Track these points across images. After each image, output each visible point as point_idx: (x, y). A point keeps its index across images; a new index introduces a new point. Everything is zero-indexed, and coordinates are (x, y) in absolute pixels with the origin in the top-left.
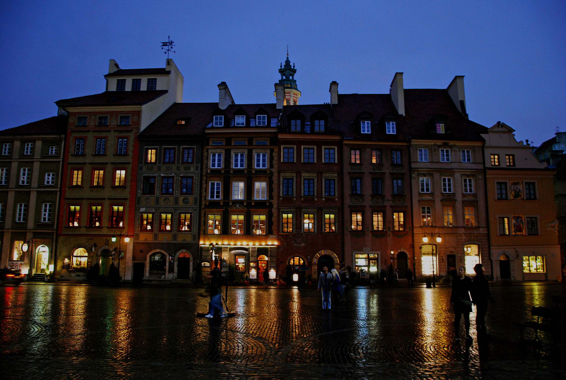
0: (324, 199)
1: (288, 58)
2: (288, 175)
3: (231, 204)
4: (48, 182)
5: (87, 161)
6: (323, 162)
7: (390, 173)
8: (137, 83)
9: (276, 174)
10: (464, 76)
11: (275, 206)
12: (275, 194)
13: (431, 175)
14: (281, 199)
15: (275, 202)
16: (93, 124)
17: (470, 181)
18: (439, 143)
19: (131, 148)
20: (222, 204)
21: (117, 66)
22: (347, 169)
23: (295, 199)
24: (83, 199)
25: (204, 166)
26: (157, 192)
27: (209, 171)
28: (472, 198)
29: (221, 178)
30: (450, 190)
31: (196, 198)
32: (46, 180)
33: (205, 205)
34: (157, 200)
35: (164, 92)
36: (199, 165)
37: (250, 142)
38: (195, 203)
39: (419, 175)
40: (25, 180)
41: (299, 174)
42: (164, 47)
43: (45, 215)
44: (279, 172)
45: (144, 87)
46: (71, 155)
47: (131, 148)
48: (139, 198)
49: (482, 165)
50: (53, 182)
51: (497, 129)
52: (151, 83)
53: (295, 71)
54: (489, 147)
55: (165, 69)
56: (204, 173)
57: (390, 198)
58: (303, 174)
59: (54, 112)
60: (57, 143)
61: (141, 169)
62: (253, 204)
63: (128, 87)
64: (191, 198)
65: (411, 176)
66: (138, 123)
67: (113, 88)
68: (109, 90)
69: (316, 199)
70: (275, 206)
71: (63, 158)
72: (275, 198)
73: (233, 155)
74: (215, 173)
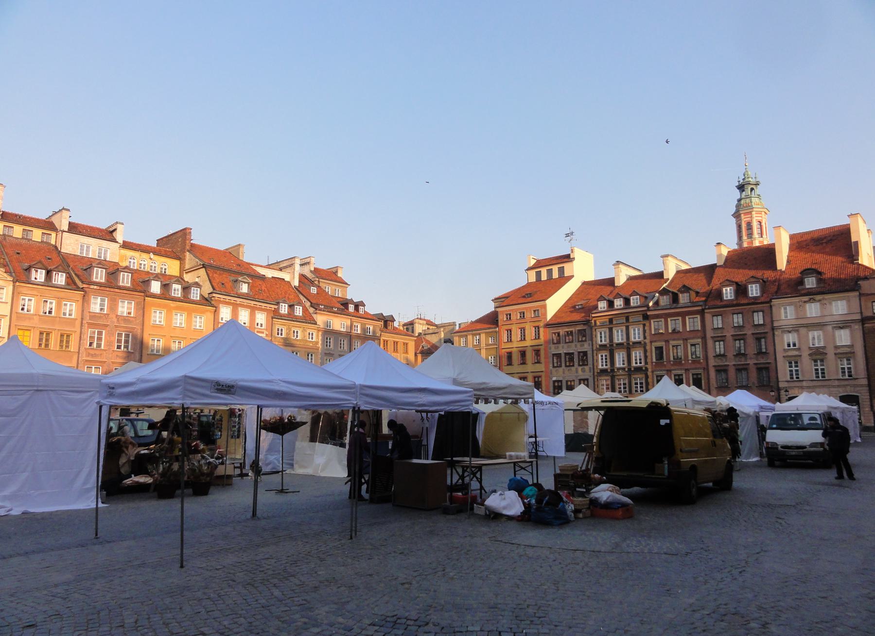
8: (550, 272)
11: (650, 370)
12: (649, 360)
13: (797, 331)
15: (649, 366)
18: (806, 298)
22: (710, 333)
26: (563, 365)
35: (572, 277)
37: (627, 319)
41: (667, 341)
44: (651, 342)
45: (555, 275)
52: (561, 270)
53: (757, 184)
59: (490, 308)
63: (544, 277)
64: (586, 368)
65: (774, 334)
66: (545, 314)
74: (603, 347)
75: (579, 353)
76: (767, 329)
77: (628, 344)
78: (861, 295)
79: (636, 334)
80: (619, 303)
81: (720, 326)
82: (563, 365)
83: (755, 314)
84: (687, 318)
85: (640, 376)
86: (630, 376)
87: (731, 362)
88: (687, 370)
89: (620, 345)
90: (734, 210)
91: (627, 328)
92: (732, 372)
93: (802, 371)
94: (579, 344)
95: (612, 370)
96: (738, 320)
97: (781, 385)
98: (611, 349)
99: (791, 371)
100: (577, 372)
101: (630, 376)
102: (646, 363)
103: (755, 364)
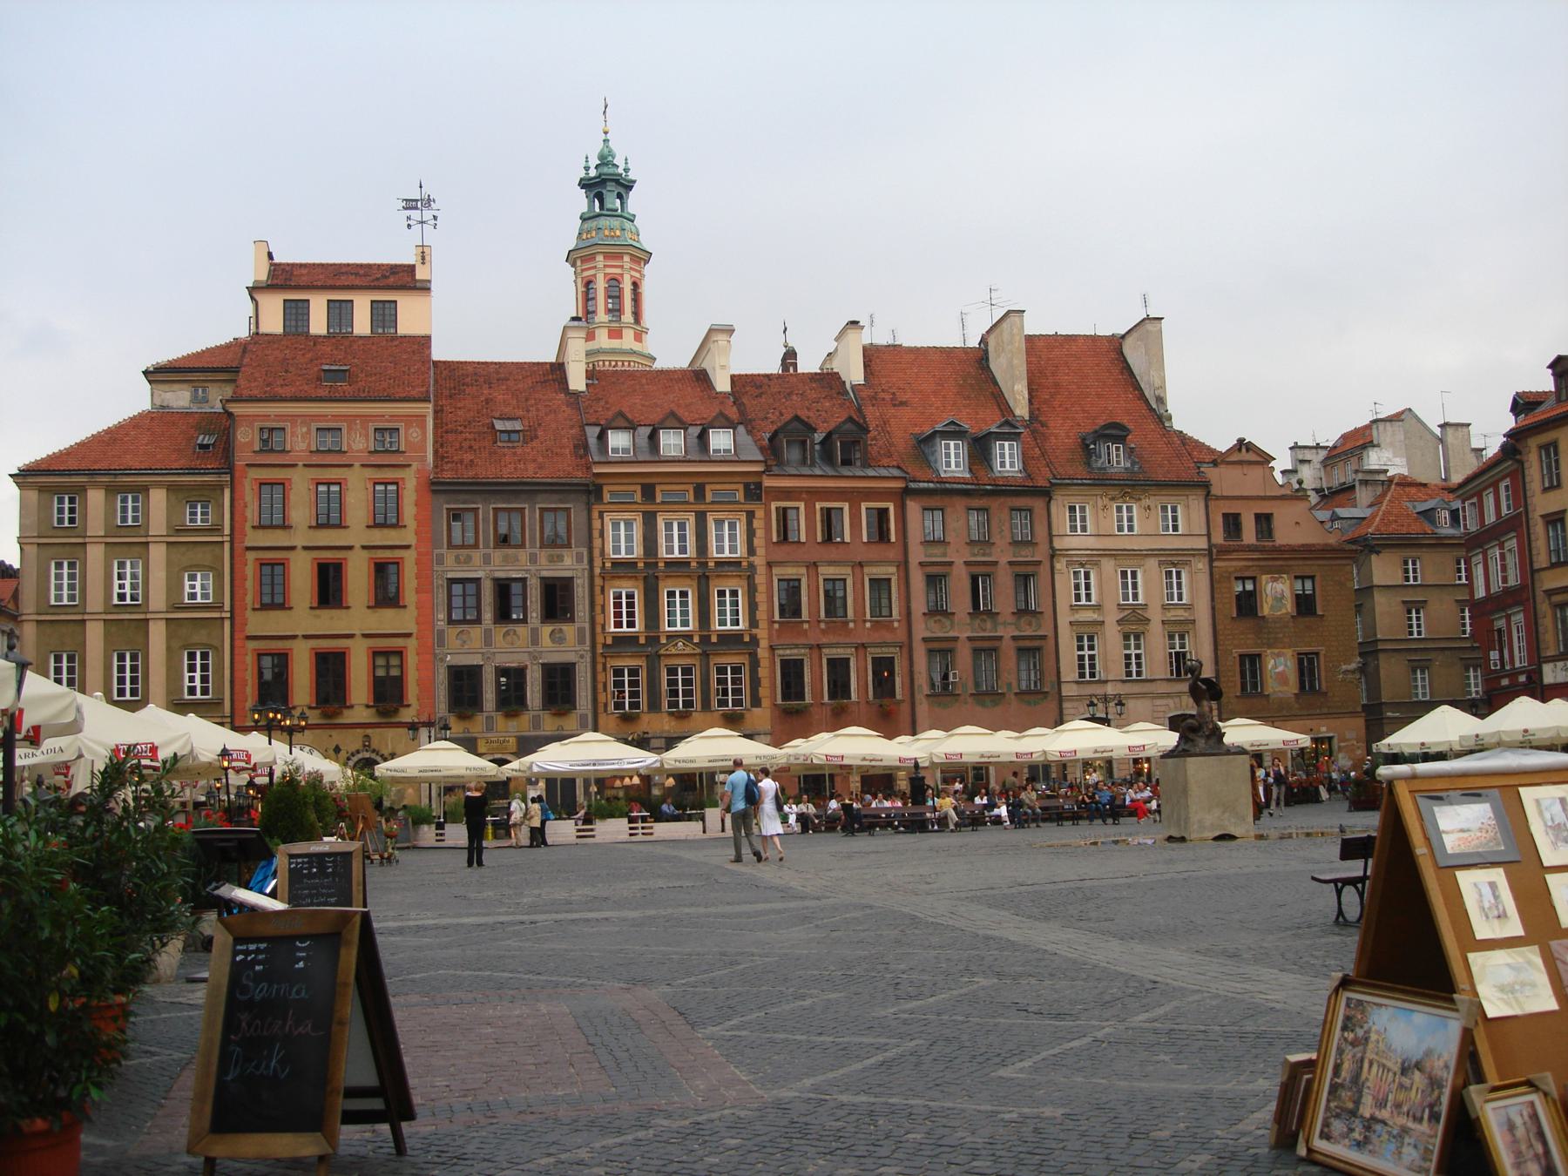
0: (868, 625)
3: (663, 641)
4: (193, 596)
5: (299, 543)
7: (1010, 563)
8: (342, 313)
9: (761, 570)
11: (764, 643)
12: (761, 615)
13: (1097, 564)
15: (762, 633)
16: (303, 446)
17: (1178, 573)
19: (409, 511)
20: (642, 641)
24: (294, 637)
25: (596, 553)
27: (608, 565)
28: (1182, 614)
31: (581, 631)
32: (187, 590)
33: (605, 645)
37: (700, 492)
38: (581, 641)
39: (1069, 564)
40: (128, 590)
43: (192, 679)
44: (770, 565)
48: (441, 633)
50: (205, 596)
53: (629, 186)
54: (1218, 498)
55: (411, 269)
56: (597, 571)
57: (1011, 619)
58: (821, 570)
59: (137, 399)
60: (205, 495)
61: (440, 561)
62: (714, 639)
64: (569, 630)
65: (1052, 568)
67: (273, 323)
68: (263, 330)
69: (851, 625)
71: (232, 535)
72: (763, 625)
73: (661, 525)
74: (623, 568)
76: (1041, 554)
79: (727, 543)
80: (672, 442)
81: (939, 534)
84: (864, 506)
85: (736, 660)
86: (705, 655)
91: (701, 519)
92: (964, 655)
93: (1105, 661)
94: (543, 555)
97: (1067, 690)
98: (650, 573)
99: (1081, 658)
100: (535, 639)
101: (705, 655)
102: (753, 623)
103: (1014, 638)
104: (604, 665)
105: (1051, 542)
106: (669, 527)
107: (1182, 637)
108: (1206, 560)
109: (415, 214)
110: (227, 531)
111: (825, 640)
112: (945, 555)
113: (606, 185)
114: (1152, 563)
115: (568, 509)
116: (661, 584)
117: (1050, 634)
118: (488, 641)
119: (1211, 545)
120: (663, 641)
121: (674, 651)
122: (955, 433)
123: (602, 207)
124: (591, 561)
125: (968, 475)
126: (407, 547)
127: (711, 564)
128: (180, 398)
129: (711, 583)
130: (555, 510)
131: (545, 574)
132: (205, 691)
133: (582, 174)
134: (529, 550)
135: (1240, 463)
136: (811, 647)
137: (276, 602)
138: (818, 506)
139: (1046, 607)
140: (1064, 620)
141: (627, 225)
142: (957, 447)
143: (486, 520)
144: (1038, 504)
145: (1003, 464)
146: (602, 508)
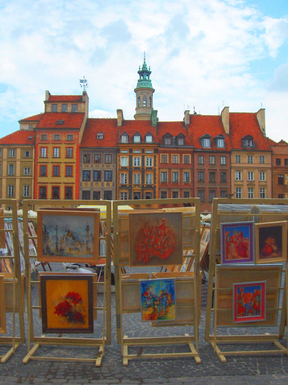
1: (145, 62)
2: (164, 170)
3: (133, 186)
6: (183, 163)
7: (220, 170)
10: (265, 109)
11: (157, 188)
12: (157, 181)
14: (160, 183)
15: (157, 185)
19: (75, 154)
20: (128, 186)
21: (49, 94)
22: (196, 167)
23: (168, 184)
24: (48, 183)
25: (118, 165)
26: (92, 179)
27: (120, 168)
28: (264, 183)
29: (127, 171)
30: (252, 179)
34: (92, 183)
36: (115, 164)
38: (113, 185)
41: (170, 169)
42: (81, 83)
44: (159, 169)
46: (40, 158)
47: (75, 154)
49: (271, 165)
51: (280, 144)
56: (118, 169)
59: (17, 128)
61: (81, 165)
62: (145, 186)
64: (111, 184)
67: (49, 110)
69: (179, 184)
70: (157, 188)
74: (124, 168)
75: (105, 171)
77: (143, 168)
78: (272, 154)
79: (149, 162)
82: (92, 179)
83: (222, 158)
84: (183, 155)
87: (207, 185)
88: (181, 189)
89: (137, 169)
90: (135, 87)
92: (207, 192)
94: (105, 165)
95: (130, 186)
96: (212, 160)
98: (130, 170)
100: (103, 185)
103: (220, 188)
104: (119, 192)
105: (231, 165)
106: (135, 159)
107: (264, 189)
108: (271, 170)
109: (82, 84)
110: (34, 158)
111: (172, 187)
112: (203, 167)
113: (144, 73)
114: (257, 171)
115: (111, 155)
116: (133, 173)
117: (229, 187)
118: (92, 185)
119: (272, 166)
120: (133, 186)
121: (135, 189)
122: (207, 137)
123: (143, 78)
124: (116, 166)
125: (210, 148)
126: (74, 163)
127: (145, 168)
128: (26, 127)
129: (145, 173)
130: (108, 155)
131: (105, 170)
132: (28, 195)
133: (139, 70)
134: (102, 164)
135: (281, 146)
136: (169, 189)
137: (44, 175)
138: (172, 155)
139: (228, 180)
140: (232, 185)
141: (149, 82)
142: (208, 141)
143: (92, 156)
144: (228, 155)
145: (220, 145)
146: (119, 154)
